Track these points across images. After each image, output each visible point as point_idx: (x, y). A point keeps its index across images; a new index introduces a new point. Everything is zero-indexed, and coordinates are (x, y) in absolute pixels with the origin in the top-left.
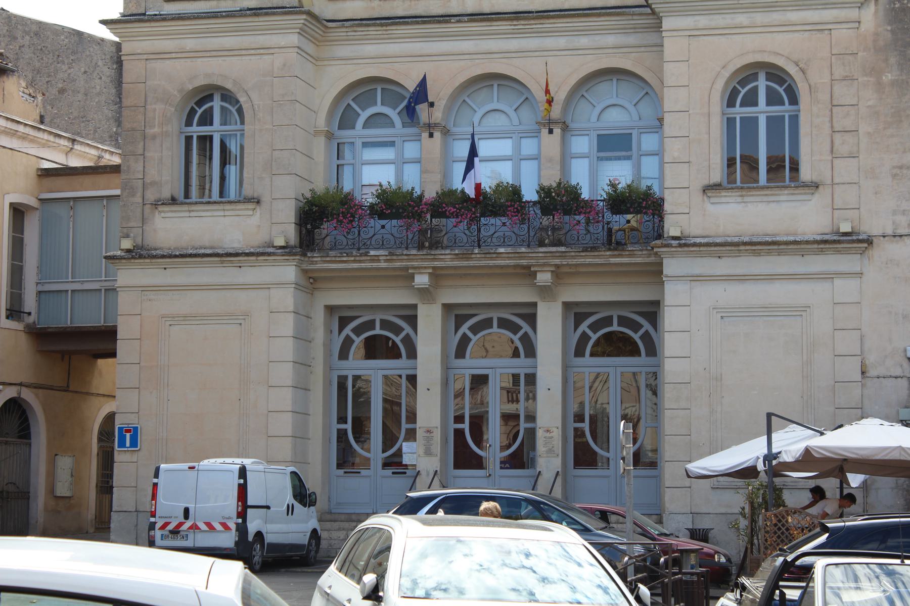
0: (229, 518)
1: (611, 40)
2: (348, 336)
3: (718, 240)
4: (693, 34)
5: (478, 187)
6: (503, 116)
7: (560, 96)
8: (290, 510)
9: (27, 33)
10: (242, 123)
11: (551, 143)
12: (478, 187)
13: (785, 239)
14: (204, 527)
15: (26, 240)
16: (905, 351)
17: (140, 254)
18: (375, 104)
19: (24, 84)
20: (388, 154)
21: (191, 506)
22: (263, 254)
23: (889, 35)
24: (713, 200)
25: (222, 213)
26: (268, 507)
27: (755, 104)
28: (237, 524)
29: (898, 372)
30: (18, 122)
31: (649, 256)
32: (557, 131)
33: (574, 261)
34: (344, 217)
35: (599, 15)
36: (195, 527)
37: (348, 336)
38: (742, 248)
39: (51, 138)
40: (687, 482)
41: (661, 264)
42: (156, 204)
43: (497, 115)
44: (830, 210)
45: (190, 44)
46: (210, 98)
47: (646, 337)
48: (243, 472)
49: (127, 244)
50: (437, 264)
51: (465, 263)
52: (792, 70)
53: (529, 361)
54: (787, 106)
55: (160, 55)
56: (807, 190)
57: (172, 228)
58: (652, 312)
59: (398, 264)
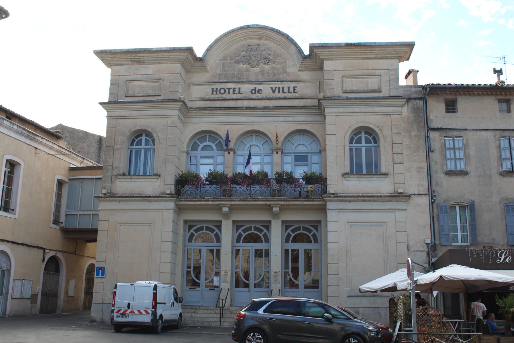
0: (149, 308)
1: (301, 119)
2: (192, 233)
3: (350, 195)
4: (338, 115)
5: (251, 171)
6: (257, 148)
7: (281, 139)
8: (173, 304)
9: (68, 132)
10: (154, 145)
11: (277, 157)
12: (251, 171)
13: (377, 195)
14: (137, 312)
15: (62, 195)
16: (425, 240)
17: (109, 196)
18: (206, 141)
19: (66, 144)
21: (131, 302)
22: (161, 197)
23: (413, 118)
24: (346, 179)
25: (144, 180)
26: (165, 303)
29: (422, 249)
30: (63, 148)
31: (320, 201)
32: (280, 153)
33: (290, 203)
34: (195, 182)
35: (297, 109)
36: (132, 312)
37: (192, 233)
38: (359, 198)
39: (75, 156)
40: (361, 294)
41: (326, 205)
42: (117, 176)
44: (393, 184)
45: (135, 113)
46: (141, 135)
48: (155, 287)
49: (104, 191)
50: (232, 203)
52: (376, 130)
53: (267, 244)
54: (373, 144)
56: (384, 176)
57: (123, 186)
58: (317, 225)
59: (216, 203)
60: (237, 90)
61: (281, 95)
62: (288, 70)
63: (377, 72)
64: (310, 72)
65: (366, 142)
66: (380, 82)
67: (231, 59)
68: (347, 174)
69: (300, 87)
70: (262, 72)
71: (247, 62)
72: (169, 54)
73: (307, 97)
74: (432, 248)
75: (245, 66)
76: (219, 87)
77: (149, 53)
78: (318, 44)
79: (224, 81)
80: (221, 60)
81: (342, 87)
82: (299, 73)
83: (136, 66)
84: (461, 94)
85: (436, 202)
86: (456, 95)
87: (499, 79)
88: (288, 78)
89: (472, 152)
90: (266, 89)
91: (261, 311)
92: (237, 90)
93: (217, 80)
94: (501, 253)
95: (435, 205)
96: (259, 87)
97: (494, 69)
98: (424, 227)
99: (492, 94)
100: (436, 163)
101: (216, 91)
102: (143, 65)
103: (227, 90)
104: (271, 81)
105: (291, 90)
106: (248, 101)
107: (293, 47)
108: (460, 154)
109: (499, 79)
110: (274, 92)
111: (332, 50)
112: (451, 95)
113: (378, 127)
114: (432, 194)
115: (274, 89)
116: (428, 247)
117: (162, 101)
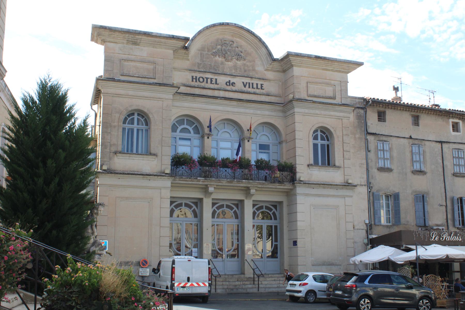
0: (206, 281)
1: (267, 113)
3: (315, 183)
6: (228, 134)
14: (196, 285)
18: (184, 124)
20: (188, 143)
21: (190, 276)
23: (357, 123)
24: (311, 169)
25: (142, 159)
27: (317, 139)
28: (209, 284)
42: (116, 153)
43: (226, 133)
45: (131, 93)
47: (274, 214)
51: (229, 184)
52: (332, 130)
55: (119, 95)
56: (337, 169)
57: (122, 162)
60: (214, 81)
61: (251, 90)
63: (333, 82)
64: (274, 73)
65: (321, 140)
66: (334, 91)
67: (209, 51)
68: (311, 165)
69: (266, 84)
70: (235, 67)
71: (223, 56)
72: (167, 40)
74: (370, 228)
75: (220, 59)
76: (198, 75)
77: (148, 37)
78: (295, 53)
79: (203, 70)
80: (199, 50)
82: (266, 72)
83: (131, 46)
84: (389, 108)
85: (372, 191)
86: (385, 108)
87: (396, 95)
88: (257, 76)
89: (395, 154)
90: (239, 82)
91: (366, 282)
92: (214, 81)
94: (433, 234)
95: (371, 193)
96: (233, 80)
97: (394, 86)
98: (364, 210)
99: (409, 111)
100: (372, 161)
101: (196, 79)
102: (137, 47)
103: (205, 80)
104: (243, 77)
105: (259, 86)
106: (224, 92)
108: (387, 155)
109: (396, 95)
110: (245, 86)
111: (303, 59)
112: (381, 108)
113: (333, 128)
114: (369, 185)
115: (245, 84)
116: (367, 226)
117: (160, 84)
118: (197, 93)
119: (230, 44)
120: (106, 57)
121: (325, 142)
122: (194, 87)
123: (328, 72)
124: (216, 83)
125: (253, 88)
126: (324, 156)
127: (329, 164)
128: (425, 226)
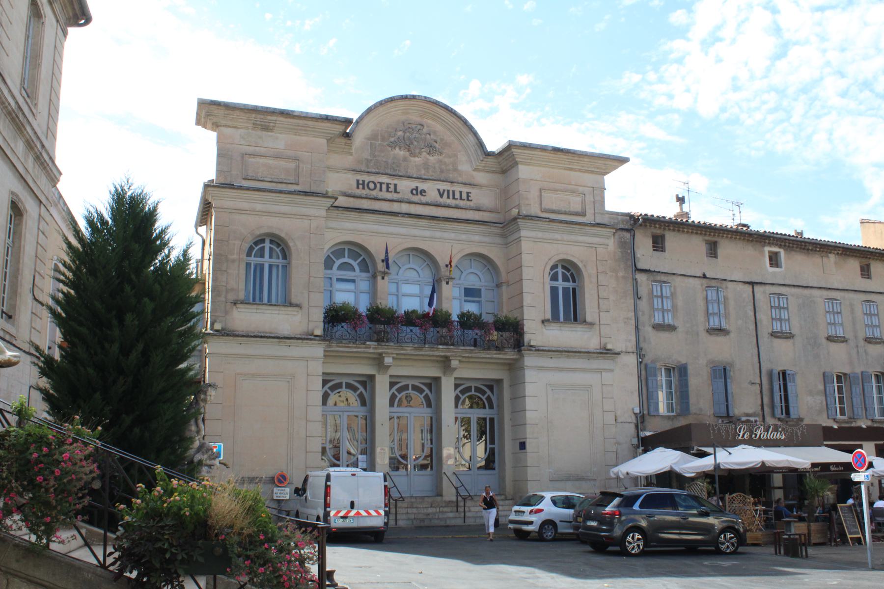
0: (380, 508)
1: (477, 238)
6: (415, 273)
14: (364, 514)
20: (350, 286)
22: (307, 339)
28: (385, 511)
29: (630, 420)
36: (358, 513)
42: (235, 303)
45: (259, 207)
47: (489, 399)
51: (417, 353)
52: (580, 265)
57: (245, 318)
61: (450, 202)
62: (460, 168)
63: (581, 189)
64: (487, 175)
65: (564, 280)
66: (584, 203)
67: (383, 139)
68: (548, 320)
69: (474, 192)
72: (316, 123)
73: (485, 208)
74: (641, 420)
79: (374, 171)
80: (368, 139)
81: (541, 204)
82: (475, 174)
83: (259, 133)
84: (669, 229)
85: (644, 362)
86: (664, 229)
87: (681, 209)
88: (460, 179)
89: (680, 303)
90: (431, 189)
91: (636, 507)
93: (364, 168)
94: (740, 428)
96: (422, 186)
97: (677, 196)
99: (701, 234)
100: (643, 314)
101: (363, 184)
103: (378, 185)
105: (464, 196)
106: (407, 205)
107: (471, 137)
108: (668, 304)
109: (681, 209)
110: (441, 196)
112: (658, 230)
114: (639, 352)
117: (306, 193)
118: (365, 207)
119: (417, 129)
120: (218, 150)
121: (570, 285)
122: (361, 197)
123: (572, 173)
124: (396, 191)
125: (454, 198)
126: (569, 306)
127: (575, 319)
128: (728, 416)
